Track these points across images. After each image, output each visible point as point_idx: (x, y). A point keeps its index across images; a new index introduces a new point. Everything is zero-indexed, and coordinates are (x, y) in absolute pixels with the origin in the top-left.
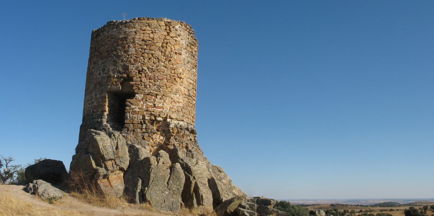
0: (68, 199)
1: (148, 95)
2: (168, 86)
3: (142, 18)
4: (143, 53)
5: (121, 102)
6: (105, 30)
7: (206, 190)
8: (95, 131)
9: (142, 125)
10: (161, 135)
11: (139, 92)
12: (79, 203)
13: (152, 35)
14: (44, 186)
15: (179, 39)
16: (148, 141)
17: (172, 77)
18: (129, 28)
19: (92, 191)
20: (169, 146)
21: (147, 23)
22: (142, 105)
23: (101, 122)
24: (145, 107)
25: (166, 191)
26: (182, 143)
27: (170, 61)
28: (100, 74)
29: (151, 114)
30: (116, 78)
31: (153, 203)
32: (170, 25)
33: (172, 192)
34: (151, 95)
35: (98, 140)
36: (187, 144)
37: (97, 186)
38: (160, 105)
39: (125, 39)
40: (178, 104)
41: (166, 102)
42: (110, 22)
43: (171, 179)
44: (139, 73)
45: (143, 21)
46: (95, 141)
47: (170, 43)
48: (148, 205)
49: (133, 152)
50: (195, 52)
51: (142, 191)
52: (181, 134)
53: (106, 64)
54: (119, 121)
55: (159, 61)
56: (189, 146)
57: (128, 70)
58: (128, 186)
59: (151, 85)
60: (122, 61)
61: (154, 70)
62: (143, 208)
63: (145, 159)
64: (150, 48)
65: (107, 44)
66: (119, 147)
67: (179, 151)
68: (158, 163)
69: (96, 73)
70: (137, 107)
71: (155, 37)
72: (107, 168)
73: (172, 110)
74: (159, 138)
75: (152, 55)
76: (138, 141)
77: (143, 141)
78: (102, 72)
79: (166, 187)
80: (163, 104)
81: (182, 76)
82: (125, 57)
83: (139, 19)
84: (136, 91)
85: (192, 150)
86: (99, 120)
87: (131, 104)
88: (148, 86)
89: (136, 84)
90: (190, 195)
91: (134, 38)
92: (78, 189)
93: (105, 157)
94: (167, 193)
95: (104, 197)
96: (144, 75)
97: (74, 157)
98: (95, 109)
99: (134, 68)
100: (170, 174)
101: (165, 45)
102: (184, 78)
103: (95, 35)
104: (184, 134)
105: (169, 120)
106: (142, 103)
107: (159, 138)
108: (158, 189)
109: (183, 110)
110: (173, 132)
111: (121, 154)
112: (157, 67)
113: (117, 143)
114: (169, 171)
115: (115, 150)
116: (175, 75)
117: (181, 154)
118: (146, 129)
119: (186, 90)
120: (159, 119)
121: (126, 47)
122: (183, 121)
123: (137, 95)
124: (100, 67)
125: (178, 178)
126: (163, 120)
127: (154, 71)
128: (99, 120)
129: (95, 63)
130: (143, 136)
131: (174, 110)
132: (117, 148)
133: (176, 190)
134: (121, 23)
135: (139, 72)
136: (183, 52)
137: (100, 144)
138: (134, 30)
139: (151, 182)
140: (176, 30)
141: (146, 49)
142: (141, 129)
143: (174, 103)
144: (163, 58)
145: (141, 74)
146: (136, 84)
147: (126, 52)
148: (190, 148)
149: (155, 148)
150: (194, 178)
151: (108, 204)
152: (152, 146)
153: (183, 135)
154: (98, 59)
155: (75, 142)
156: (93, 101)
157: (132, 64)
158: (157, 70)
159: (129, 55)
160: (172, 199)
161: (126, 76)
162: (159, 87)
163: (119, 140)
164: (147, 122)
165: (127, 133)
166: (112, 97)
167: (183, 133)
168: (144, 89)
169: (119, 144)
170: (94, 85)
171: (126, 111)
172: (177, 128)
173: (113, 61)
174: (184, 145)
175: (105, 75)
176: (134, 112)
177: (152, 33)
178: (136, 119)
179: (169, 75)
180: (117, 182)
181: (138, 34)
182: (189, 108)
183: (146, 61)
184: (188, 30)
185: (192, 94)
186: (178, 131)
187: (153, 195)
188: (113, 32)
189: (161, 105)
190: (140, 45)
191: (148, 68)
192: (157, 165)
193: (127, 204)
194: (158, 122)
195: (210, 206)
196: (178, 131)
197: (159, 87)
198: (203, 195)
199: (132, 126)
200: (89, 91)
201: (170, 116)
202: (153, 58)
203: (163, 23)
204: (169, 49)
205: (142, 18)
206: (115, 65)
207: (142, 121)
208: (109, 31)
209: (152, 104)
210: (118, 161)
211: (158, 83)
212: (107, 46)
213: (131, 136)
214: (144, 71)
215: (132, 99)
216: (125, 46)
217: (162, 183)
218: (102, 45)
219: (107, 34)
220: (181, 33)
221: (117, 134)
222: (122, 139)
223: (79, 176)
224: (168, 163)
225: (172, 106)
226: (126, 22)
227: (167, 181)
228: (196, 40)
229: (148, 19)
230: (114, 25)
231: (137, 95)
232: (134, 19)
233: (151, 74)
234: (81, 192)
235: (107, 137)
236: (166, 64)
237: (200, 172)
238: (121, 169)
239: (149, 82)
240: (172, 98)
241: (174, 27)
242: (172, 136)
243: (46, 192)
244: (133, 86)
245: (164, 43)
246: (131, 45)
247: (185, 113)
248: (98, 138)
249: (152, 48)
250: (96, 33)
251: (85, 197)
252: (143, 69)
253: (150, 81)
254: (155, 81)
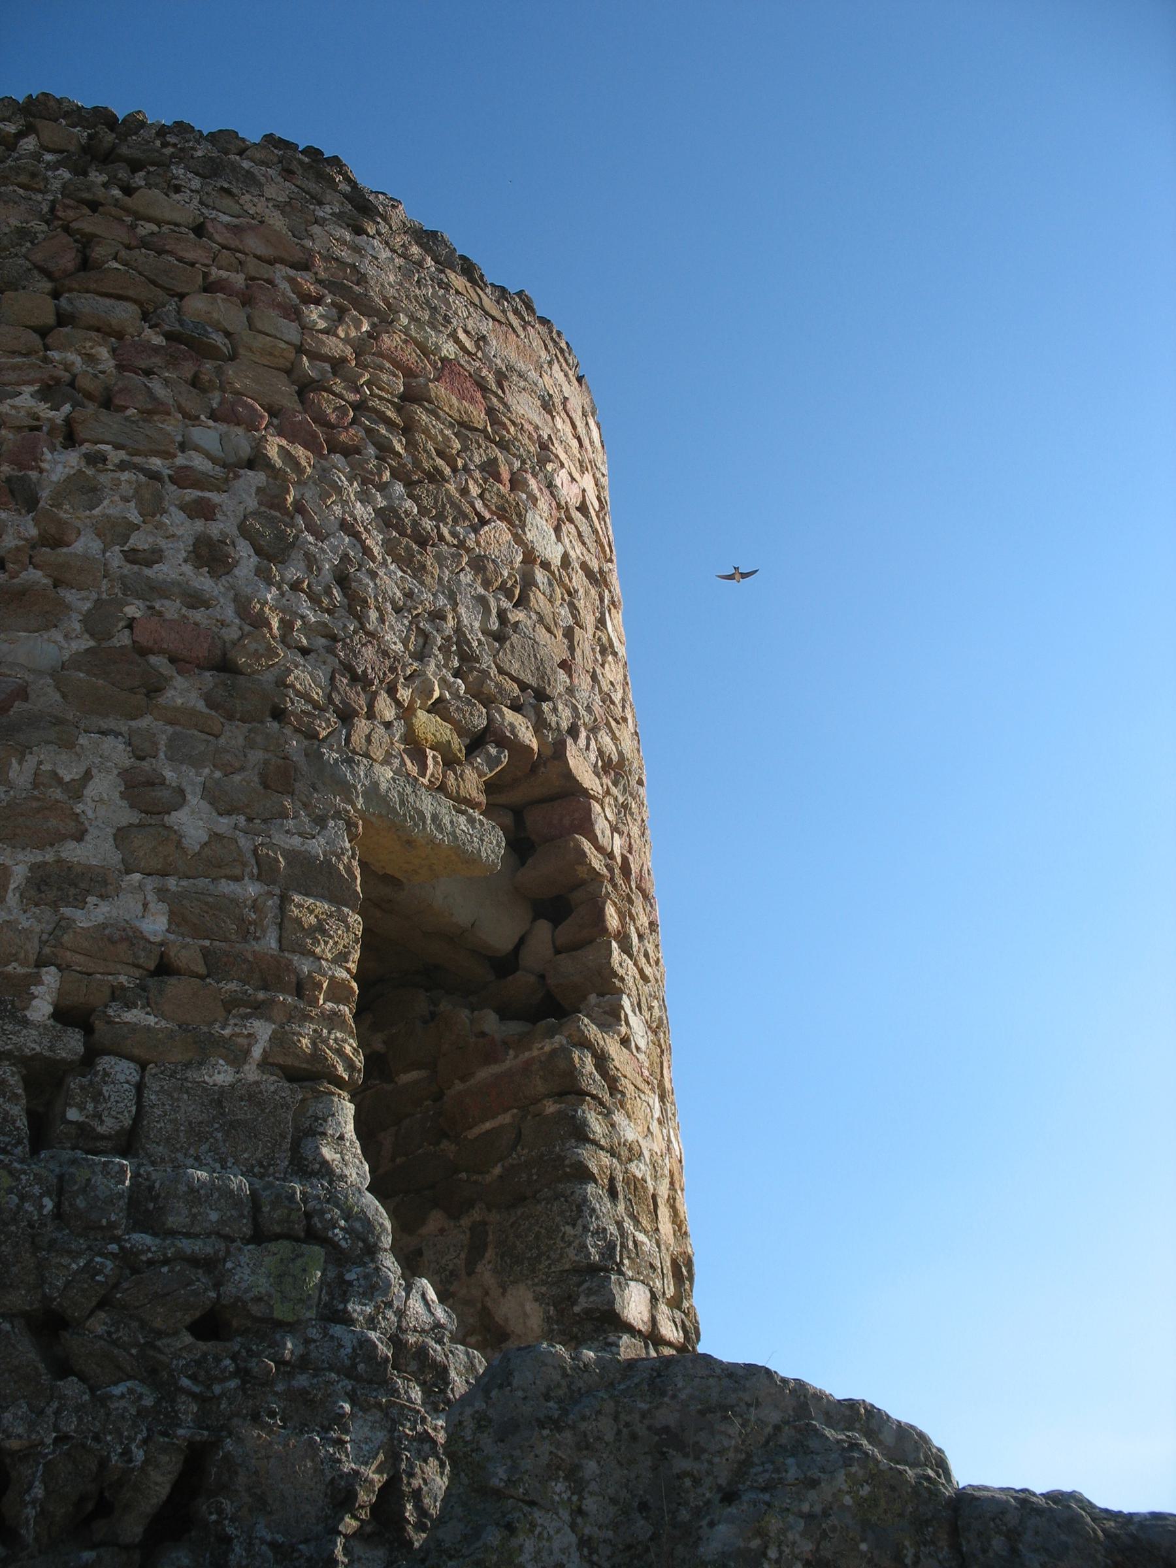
156: (73, 852)
219: (277, 221)
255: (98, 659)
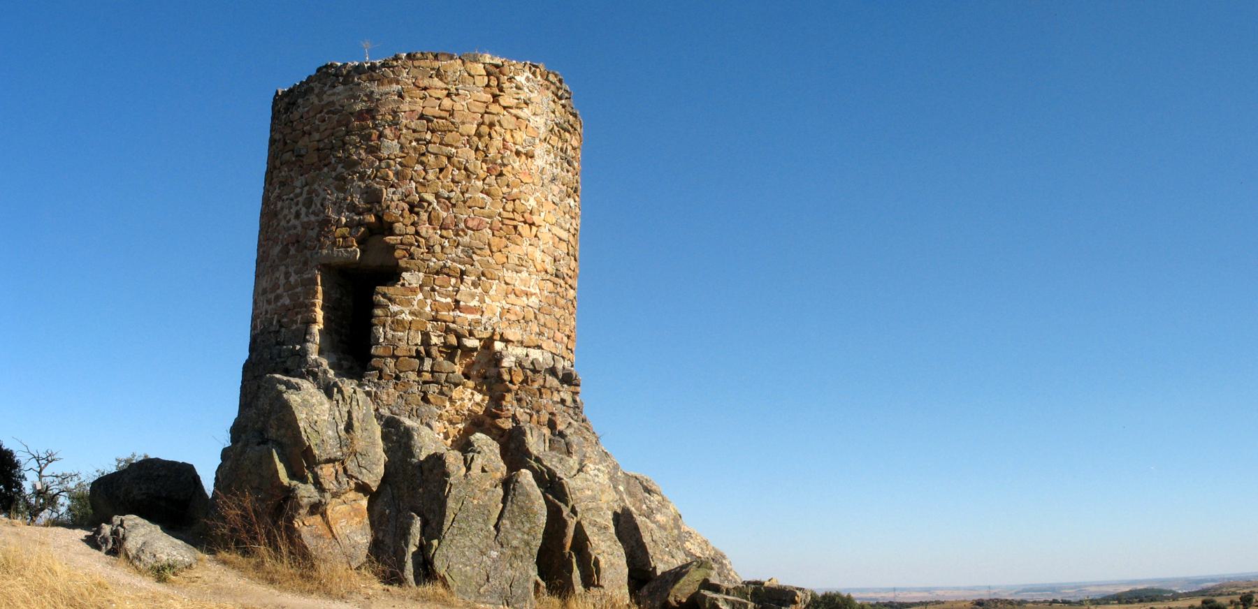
0: (210, 570)
1: (437, 273)
2: (494, 249)
3: (419, 55)
4: (423, 154)
5: (359, 293)
6: (312, 89)
7: (609, 543)
8: (285, 378)
9: (422, 360)
10: (475, 388)
11: (413, 266)
12: (241, 582)
13: (447, 103)
14: (141, 532)
15: (525, 113)
16: (439, 407)
17: (506, 222)
18: (381, 82)
19: (276, 549)
20: (500, 422)
21: (433, 69)
22: (422, 304)
23: (304, 354)
24: (428, 309)
25: (491, 548)
26: (538, 412)
27: (501, 174)
28: (298, 215)
29: (448, 330)
30: (346, 225)
31: (455, 584)
32: (501, 72)
33: (508, 552)
34: (448, 275)
35: (294, 405)
36: (552, 414)
37: (292, 535)
38: (472, 304)
39: (371, 113)
40: (524, 298)
41: (492, 292)
42: (326, 66)
43: (506, 514)
44: (411, 211)
45: (422, 63)
46: (286, 408)
47: (501, 125)
48: (441, 590)
49: (397, 438)
50: (574, 149)
51: (423, 549)
52: (536, 386)
53: (316, 186)
54: (355, 350)
55: (468, 177)
56: (559, 420)
57: (379, 202)
58: (380, 535)
59: (447, 244)
60: (361, 178)
61: (453, 201)
62: (424, 599)
63: (429, 457)
64: (442, 139)
65: (317, 130)
66: (356, 424)
67: (529, 436)
68: (468, 469)
69: (286, 212)
70: (407, 309)
71: (457, 107)
72: (321, 484)
73: (508, 316)
74: (470, 399)
75: (449, 158)
76: (409, 408)
77: (424, 408)
78: (304, 210)
79: (492, 537)
80: (482, 301)
81: (535, 218)
82: (371, 166)
83: (409, 56)
84: (402, 263)
85: (568, 432)
86: (298, 347)
87: (390, 300)
88: (437, 248)
89: (402, 243)
90: (561, 560)
91: (395, 112)
92: (237, 543)
93: (316, 452)
94: (494, 554)
95: (313, 565)
96: (424, 216)
97: (225, 454)
98: (285, 316)
99: (395, 198)
100: (504, 501)
101: (485, 129)
102: (543, 224)
103: (282, 105)
104: (544, 387)
105: (498, 346)
106: (420, 296)
107: (470, 399)
108: (468, 543)
109: (540, 316)
110: (511, 382)
111: (360, 445)
112: (463, 193)
113: (349, 413)
114: (500, 491)
115: (343, 433)
116: (517, 216)
117: (535, 443)
118: (432, 372)
119: (549, 259)
120: (470, 343)
121: (374, 137)
122: (539, 347)
123: (405, 275)
124: (297, 196)
125: (527, 513)
126: (483, 347)
127: (454, 205)
128: (298, 347)
129: (283, 184)
130: (425, 393)
131: (513, 318)
132: (349, 427)
133: (522, 546)
134: (359, 70)
135: (412, 208)
136: (539, 150)
137: (301, 416)
138: (395, 87)
139: (447, 524)
140: (518, 88)
141: (430, 142)
142: (420, 373)
143: (513, 296)
144: (480, 168)
145: (417, 214)
146: (402, 243)
147: (373, 150)
148: (561, 427)
149: (461, 426)
150: (574, 511)
151: (325, 586)
152: (450, 422)
153: (539, 390)
154: (292, 174)
155: (230, 410)
156: (279, 292)
157: (392, 186)
158: (464, 202)
159: (380, 160)
160: (509, 573)
161: (373, 219)
162: (470, 251)
163: (354, 403)
164: (434, 351)
165: (377, 385)
166: (332, 280)
167: (541, 382)
168: (426, 256)
169: (354, 415)
170: (282, 247)
171: (374, 321)
172: (523, 368)
173: (336, 178)
174: (545, 417)
175: (313, 218)
176: (398, 324)
177: (449, 95)
178: (403, 344)
179: (500, 215)
180: (348, 524)
181: (408, 99)
182: (556, 309)
183: (431, 176)
184: (553, 88)
185: (564, 270)
186: (526, 377)
187: (454, 560)
188: (334, 94)
189: (474, 303)
190: (414, 131)
191: (437, 196)
192: (466, 476)
193: (378, 586)
194: (469, 351)
195: (620, 588)
196: (526, 377)
197: (470, 251)
198: (600, 558)
199: (392, 365)
200: (268, 264)
201: (502, 335)
202: (450, 168)
203: (479, 69)
204: (497, 142)
205: (419, 55)
206: (341, 189)
207: (422, 349)
208: (322, 92)
209: (449, 300)
210: (351, 466)
211: (466, 239)
212: (316, 136)
213: (389, 394)
214: (425, 204)
215: (393, 285)
216: (370, 135)
217: (480, 526)
218: (304, 133)
219: (316, 102)
220: (532, 95)
221: (349, 386)
222: (365, 402)
223: (240, 507)
224: (497, 469)
225: (507, 306)
226: (373, 67)
227: (494, 521)
228: (575, 115)
229: (436, 57)
230: (336, 75)
231: (404, 274)
232: (396, 58)
233: (445, 214)
234: (246, 553)
235: (320, 396)
236: (490, 185)
237: (589, 493)
238: (362, 488)
239: (441, 236)
240: (506, 284)
241: (511, 79)
242: (509, 391)
243: (147, 551)
244: (393, 248)
245: (483, 123)
246: (387, 132)
247: (545, 326)
248: (293, 398)
249: (449, 138)
250: (286, 100)
251: (259, 566)
252: (422, 200)
253: (444, 233)
254: (457, 235)
255: (281, 251)
